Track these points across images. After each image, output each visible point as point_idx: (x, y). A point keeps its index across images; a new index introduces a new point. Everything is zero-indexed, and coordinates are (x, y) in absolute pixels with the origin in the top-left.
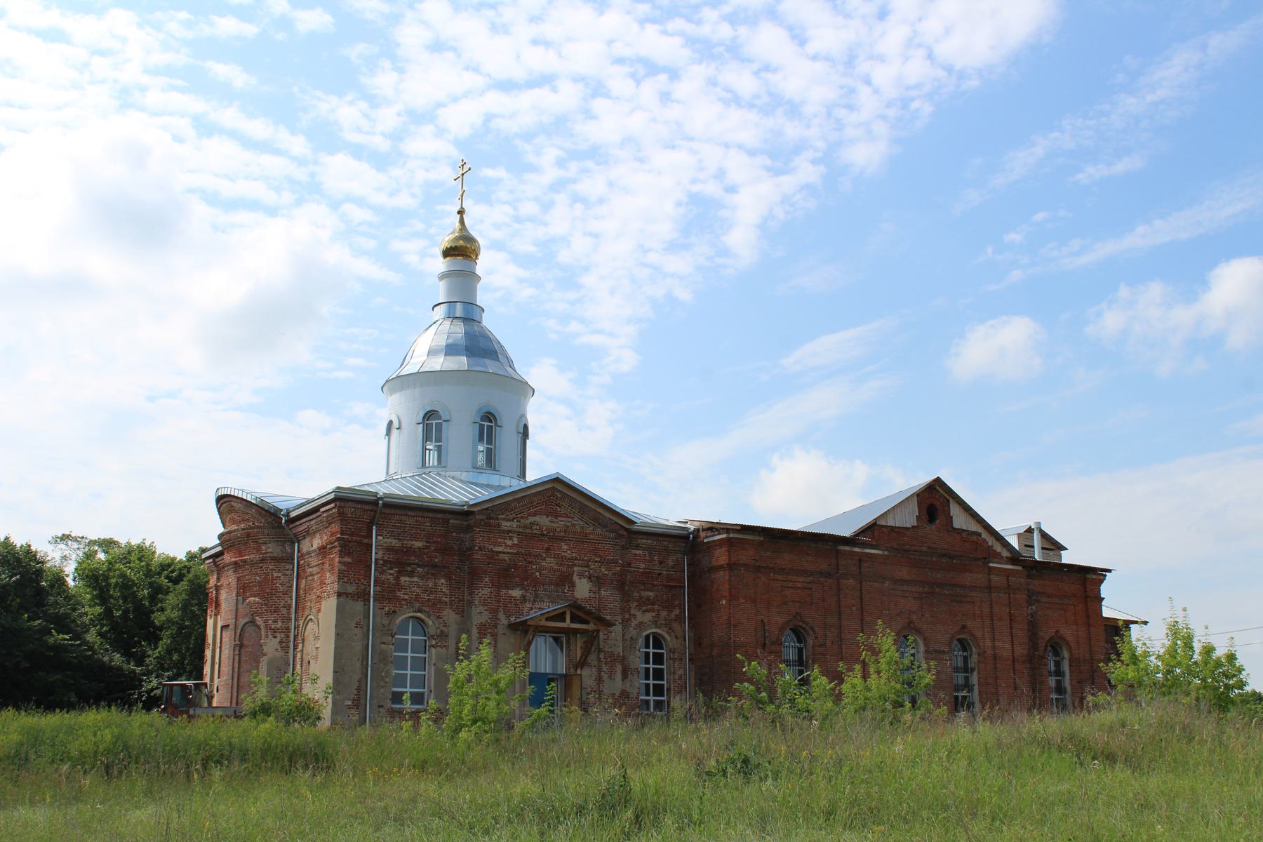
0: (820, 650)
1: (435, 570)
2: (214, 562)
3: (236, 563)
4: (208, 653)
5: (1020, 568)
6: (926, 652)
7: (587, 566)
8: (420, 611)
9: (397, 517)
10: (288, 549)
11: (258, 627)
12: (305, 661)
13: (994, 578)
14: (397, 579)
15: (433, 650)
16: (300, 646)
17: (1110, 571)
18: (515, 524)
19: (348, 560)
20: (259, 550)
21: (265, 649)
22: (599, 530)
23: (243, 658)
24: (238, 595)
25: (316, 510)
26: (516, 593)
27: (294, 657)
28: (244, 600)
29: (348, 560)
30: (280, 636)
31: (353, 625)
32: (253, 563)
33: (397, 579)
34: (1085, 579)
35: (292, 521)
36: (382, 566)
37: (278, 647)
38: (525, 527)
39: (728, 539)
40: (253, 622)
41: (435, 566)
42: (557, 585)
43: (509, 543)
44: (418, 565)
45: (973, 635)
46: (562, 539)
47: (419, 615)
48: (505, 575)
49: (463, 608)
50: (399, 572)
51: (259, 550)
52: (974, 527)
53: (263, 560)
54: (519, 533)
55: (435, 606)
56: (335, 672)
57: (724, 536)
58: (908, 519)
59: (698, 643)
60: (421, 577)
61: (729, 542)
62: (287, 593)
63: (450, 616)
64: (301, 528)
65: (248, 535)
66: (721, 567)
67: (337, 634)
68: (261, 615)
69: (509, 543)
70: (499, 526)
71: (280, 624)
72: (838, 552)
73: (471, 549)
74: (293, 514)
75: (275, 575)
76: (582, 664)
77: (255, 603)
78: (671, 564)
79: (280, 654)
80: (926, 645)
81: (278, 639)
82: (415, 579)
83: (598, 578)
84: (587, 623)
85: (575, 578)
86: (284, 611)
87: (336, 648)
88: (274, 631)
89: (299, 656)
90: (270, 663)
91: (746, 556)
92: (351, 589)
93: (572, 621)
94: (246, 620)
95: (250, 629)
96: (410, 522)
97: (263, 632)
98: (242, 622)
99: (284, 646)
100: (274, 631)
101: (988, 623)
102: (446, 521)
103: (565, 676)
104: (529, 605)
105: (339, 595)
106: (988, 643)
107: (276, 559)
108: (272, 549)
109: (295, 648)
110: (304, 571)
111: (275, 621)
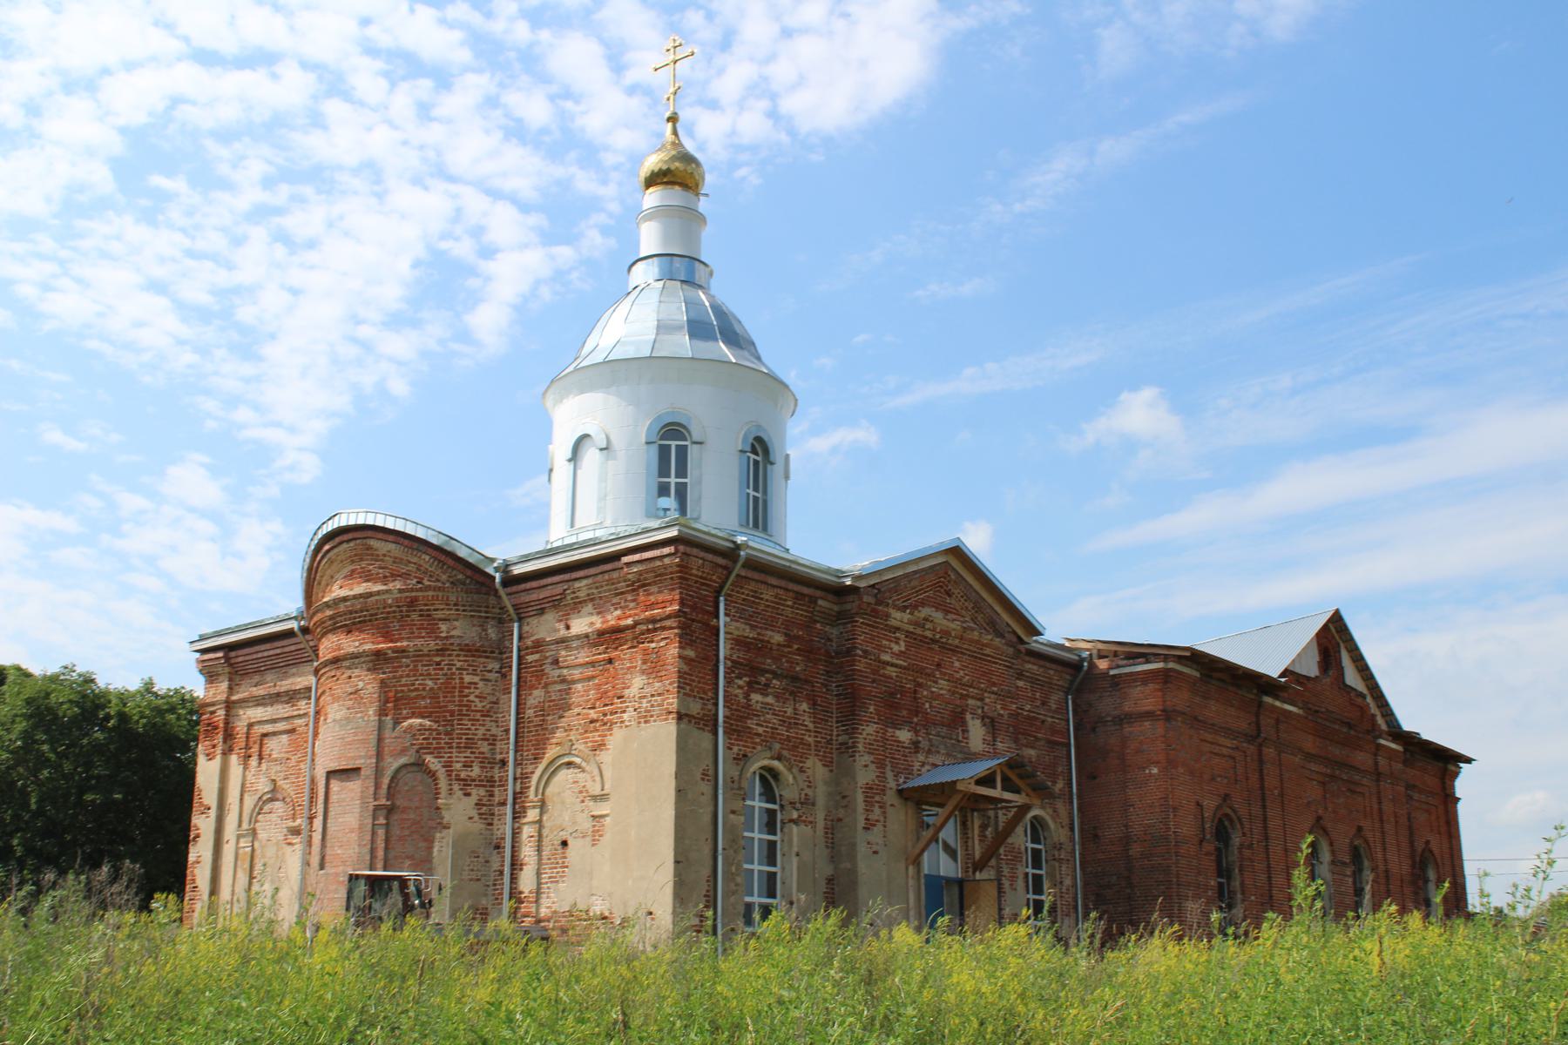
0: (1247, 853)
1: (796, 685)
2: (227, 658)
3: (378, 654)
4: (203, 824)
5: (1400, 748)
6: (1333, 862)
7: (982, 700)
8: (779, 758)
9: (752, 586)
10: (492, 633)
11: (433, 775)
12: (552, 838)
13: (1382, 761)
14: (747, 696)
15: (795, 829)
16: (532, 814)
17: (1469, 760)
18: (906, 616)
19: (690, 653)
20: (433, 631)
21: (447, 816)
22: (997, 641)
23: (396, 831)
24: (382, 712)
25: (616, 556)
26: (904, 735)
27: (516, 834)
28: (397, 723)
29: (690, 653)
30: (477, 793)
31: (699, 776)
32: (419, 655)
33: (747, 696)
34: (1446, 770)
35: (511, 581)
36: (735, 666)
37: (474, 813)
38: (916, 624)
39: (1166, 672)
40: (419, 765)
41: (795, 679)
42: (949, 726)
43: (896, 648)
44: (775, 675)
45: (1366, 841)
46: (954, 650)
47: (776, 764)
48: (900, 705)
49: (839, 754)
50: (749, 684)
51: (433, 631)
52: (1360, 686)
53: (441, 651)
54: (908, 634)
55: (794, 750)
56: (677, 862)
57: (1160, 665)
58: (1311, 669)
59: (1091, 835)
60: (777, 697)
61: (1165, 677)
62: (491, 711)
63: (816, 768)
64: (534, 596)
65: (413, 602)
66: (1149, 715)
67: (679, 791)
68: (437, 752)
69: (896, 648)
70: (888, 616)
71: (476, 771)
72: (1260, 704)
73: (849, 652)
74: (518, 570)
75: (467, 679)
76: (979, 866)
77: (422, 729)
78: (1054, 706)
79: (478, 826)
80: (1333, 852)
81: (474, 799)
82: (770, 699)
83: (993, 720)
84: (1017, 791)
85: (968, 717)
86: (484, 747)
87: (678, 817)
88: (466, 783)
89: (527, 831)
90: (457, 845)
91: (1180, 699)
92: (695, 708)
93: (1004, 789)
94: (403, 760)
95: (411, 779)
96: (768, 594)
97: (443, 783)
98: (393, 764)
99: (487, 812)
100: (466, 783)
101: (1377, 825)
102: (813, 600)
103: (960, 883)
104: (921, 757)
105: (680, 717)
106: (1380, 856)
107: (470, 650)
108: (461, 629)
109: (517, 815)
110: (540, 674)
111: (467, 765)
